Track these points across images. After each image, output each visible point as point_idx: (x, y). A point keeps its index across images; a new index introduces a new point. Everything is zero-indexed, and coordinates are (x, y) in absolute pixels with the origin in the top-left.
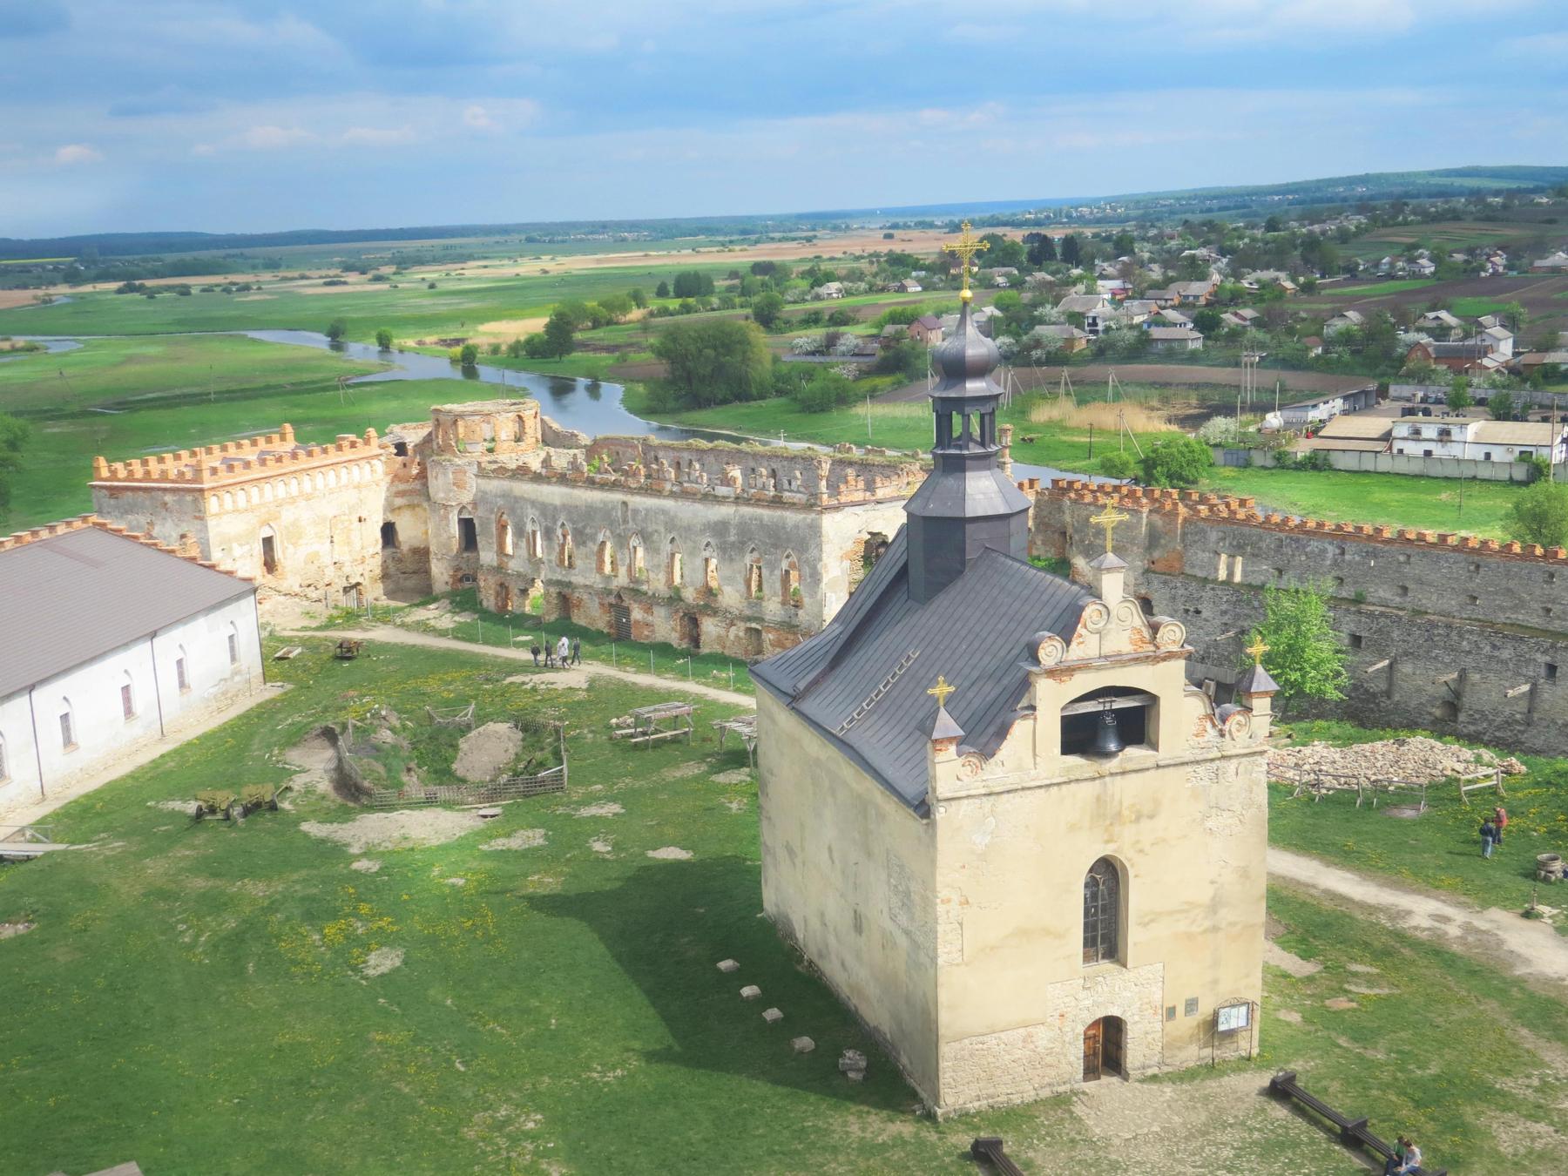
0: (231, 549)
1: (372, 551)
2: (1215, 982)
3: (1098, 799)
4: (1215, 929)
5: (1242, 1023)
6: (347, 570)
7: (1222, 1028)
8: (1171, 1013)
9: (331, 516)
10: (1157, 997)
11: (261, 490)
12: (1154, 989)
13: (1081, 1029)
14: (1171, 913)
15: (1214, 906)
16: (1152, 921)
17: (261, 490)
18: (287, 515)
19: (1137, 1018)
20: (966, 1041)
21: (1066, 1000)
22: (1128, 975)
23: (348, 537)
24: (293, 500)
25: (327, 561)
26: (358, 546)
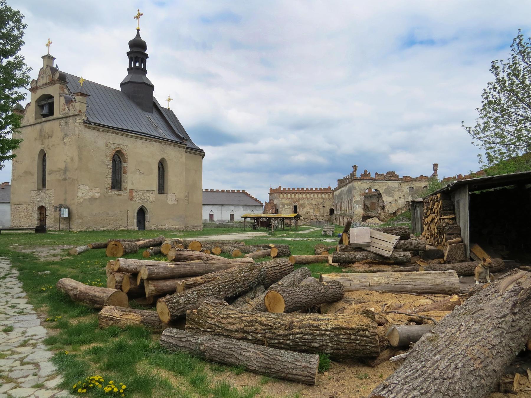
0: (284, 206)
1: (326, 214)
2: (65, 200)
3: (41, 130)
4: (65, 179)
5: (67, 216)
6: (318, 217)
7: (62, 216)
8: (56, 207)
9: (314, 204)
10: (53, 202)
11: (295, 195)
12: (52, 199)
13: (37, 208)
14: (55, 171)
15: (66, 170)
16: (51, 173)
17: (295, 195)
18: (301, 202)
19: (49, 208)
20: (16, 206)
21: (34, 197)
22: (47, 192)
23: (319, 210)
24: (303, 199)
25: (312, 214)
26: (322, 213)
